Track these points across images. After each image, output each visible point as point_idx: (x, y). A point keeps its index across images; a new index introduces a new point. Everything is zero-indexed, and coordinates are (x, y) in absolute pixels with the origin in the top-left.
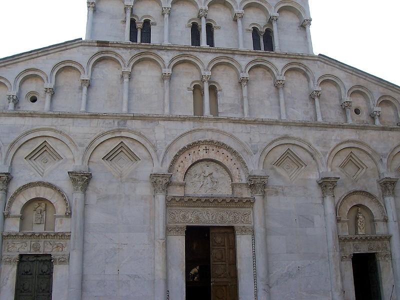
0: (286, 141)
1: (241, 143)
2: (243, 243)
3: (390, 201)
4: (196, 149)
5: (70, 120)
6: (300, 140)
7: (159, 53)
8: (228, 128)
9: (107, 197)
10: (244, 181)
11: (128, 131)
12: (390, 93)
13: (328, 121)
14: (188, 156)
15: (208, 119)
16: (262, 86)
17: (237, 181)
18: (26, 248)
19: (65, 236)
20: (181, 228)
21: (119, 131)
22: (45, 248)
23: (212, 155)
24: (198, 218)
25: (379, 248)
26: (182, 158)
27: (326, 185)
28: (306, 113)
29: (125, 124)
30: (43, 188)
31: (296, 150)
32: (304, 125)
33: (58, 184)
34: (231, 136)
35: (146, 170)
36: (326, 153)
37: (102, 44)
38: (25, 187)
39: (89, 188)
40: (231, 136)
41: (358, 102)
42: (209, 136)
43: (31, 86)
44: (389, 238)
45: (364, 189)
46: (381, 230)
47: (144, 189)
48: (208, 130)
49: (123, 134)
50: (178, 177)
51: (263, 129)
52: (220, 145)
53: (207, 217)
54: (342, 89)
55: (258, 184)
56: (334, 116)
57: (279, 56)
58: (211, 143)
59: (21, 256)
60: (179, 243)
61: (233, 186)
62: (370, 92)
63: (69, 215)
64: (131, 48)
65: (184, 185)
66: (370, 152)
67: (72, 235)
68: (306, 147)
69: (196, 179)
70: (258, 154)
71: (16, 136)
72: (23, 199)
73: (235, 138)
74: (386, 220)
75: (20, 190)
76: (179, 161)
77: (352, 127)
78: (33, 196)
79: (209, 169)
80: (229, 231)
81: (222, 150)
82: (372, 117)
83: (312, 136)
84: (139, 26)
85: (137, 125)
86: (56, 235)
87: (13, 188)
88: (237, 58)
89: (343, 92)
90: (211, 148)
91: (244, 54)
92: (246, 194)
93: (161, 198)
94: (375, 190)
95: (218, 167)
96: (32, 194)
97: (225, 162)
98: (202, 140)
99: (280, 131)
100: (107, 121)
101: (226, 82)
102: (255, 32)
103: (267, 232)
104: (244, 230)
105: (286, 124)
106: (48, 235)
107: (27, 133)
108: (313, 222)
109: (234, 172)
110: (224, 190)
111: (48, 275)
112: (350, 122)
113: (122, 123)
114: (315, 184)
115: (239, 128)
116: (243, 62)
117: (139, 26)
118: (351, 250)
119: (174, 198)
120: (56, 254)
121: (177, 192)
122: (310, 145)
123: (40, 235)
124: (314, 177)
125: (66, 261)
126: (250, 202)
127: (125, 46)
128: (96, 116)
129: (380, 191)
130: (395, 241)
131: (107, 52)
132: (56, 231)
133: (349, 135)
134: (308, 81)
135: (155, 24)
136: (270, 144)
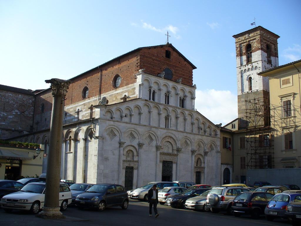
1: (176, 137)
2: (174, 166)
5: (138, 126)
6: (189, 137)
7: (160, 105)
8: (174, 132)
10: (176, 149)
11: (152, 131)
16: (181, 119)
18: (127, 164)
19: (137, 162)
21: (150, 131)
22: (132, 165)
23: (169, 140)
24: (165, 158)
27: (193, 152)
28: (190, 129)
31: (188, 141)
32: (191, 133)
33: (135, 146)
34: (174, 135)
35: (154, 143)
37: (146, 100)
40: (174, 135)
41: (202, 126)
42: (170, 135)
44: (204, 168)
47: (154, 149)
48: (169, 133)
49: (151, 132)
51: (182, 134)
52: (171, 137)
53: (168, 158)
55: (178, 150)
56: (195, 130)
57: (187, 110)
60: (161, 165)
61: (173, 150)
62: (206, 124)
63: (138, 156)
64: (153, 103)
66: (203, 143)
72: (126, 150)
73: (175, 136)
74: (204, 163)
77: (201, 135)
79: (168, 144)
80: (171, 162)
81: (171, 139)
82: (205, 131)
83: (192, 136)
86: (136, 161)
88: (177, 110)
90: (169, 138)
91: (179, 109)
96: (128, 148)
97: (172, 143)
99: (185, 134)
100: (147, 127)
102: (180, 99)
104: (175, 163)
105: (187, 133)
109: (174, 146)
111: (132, 173)
112: (201, 133)
116: (179, 111)
120: (135, 167)
121: (161, 151)
122: (191, 139)
124: (190, 149)
126: (177, 155)
130: (206, 169)
133: (200, 137)
134: (192, 118)
135: (156, 93)
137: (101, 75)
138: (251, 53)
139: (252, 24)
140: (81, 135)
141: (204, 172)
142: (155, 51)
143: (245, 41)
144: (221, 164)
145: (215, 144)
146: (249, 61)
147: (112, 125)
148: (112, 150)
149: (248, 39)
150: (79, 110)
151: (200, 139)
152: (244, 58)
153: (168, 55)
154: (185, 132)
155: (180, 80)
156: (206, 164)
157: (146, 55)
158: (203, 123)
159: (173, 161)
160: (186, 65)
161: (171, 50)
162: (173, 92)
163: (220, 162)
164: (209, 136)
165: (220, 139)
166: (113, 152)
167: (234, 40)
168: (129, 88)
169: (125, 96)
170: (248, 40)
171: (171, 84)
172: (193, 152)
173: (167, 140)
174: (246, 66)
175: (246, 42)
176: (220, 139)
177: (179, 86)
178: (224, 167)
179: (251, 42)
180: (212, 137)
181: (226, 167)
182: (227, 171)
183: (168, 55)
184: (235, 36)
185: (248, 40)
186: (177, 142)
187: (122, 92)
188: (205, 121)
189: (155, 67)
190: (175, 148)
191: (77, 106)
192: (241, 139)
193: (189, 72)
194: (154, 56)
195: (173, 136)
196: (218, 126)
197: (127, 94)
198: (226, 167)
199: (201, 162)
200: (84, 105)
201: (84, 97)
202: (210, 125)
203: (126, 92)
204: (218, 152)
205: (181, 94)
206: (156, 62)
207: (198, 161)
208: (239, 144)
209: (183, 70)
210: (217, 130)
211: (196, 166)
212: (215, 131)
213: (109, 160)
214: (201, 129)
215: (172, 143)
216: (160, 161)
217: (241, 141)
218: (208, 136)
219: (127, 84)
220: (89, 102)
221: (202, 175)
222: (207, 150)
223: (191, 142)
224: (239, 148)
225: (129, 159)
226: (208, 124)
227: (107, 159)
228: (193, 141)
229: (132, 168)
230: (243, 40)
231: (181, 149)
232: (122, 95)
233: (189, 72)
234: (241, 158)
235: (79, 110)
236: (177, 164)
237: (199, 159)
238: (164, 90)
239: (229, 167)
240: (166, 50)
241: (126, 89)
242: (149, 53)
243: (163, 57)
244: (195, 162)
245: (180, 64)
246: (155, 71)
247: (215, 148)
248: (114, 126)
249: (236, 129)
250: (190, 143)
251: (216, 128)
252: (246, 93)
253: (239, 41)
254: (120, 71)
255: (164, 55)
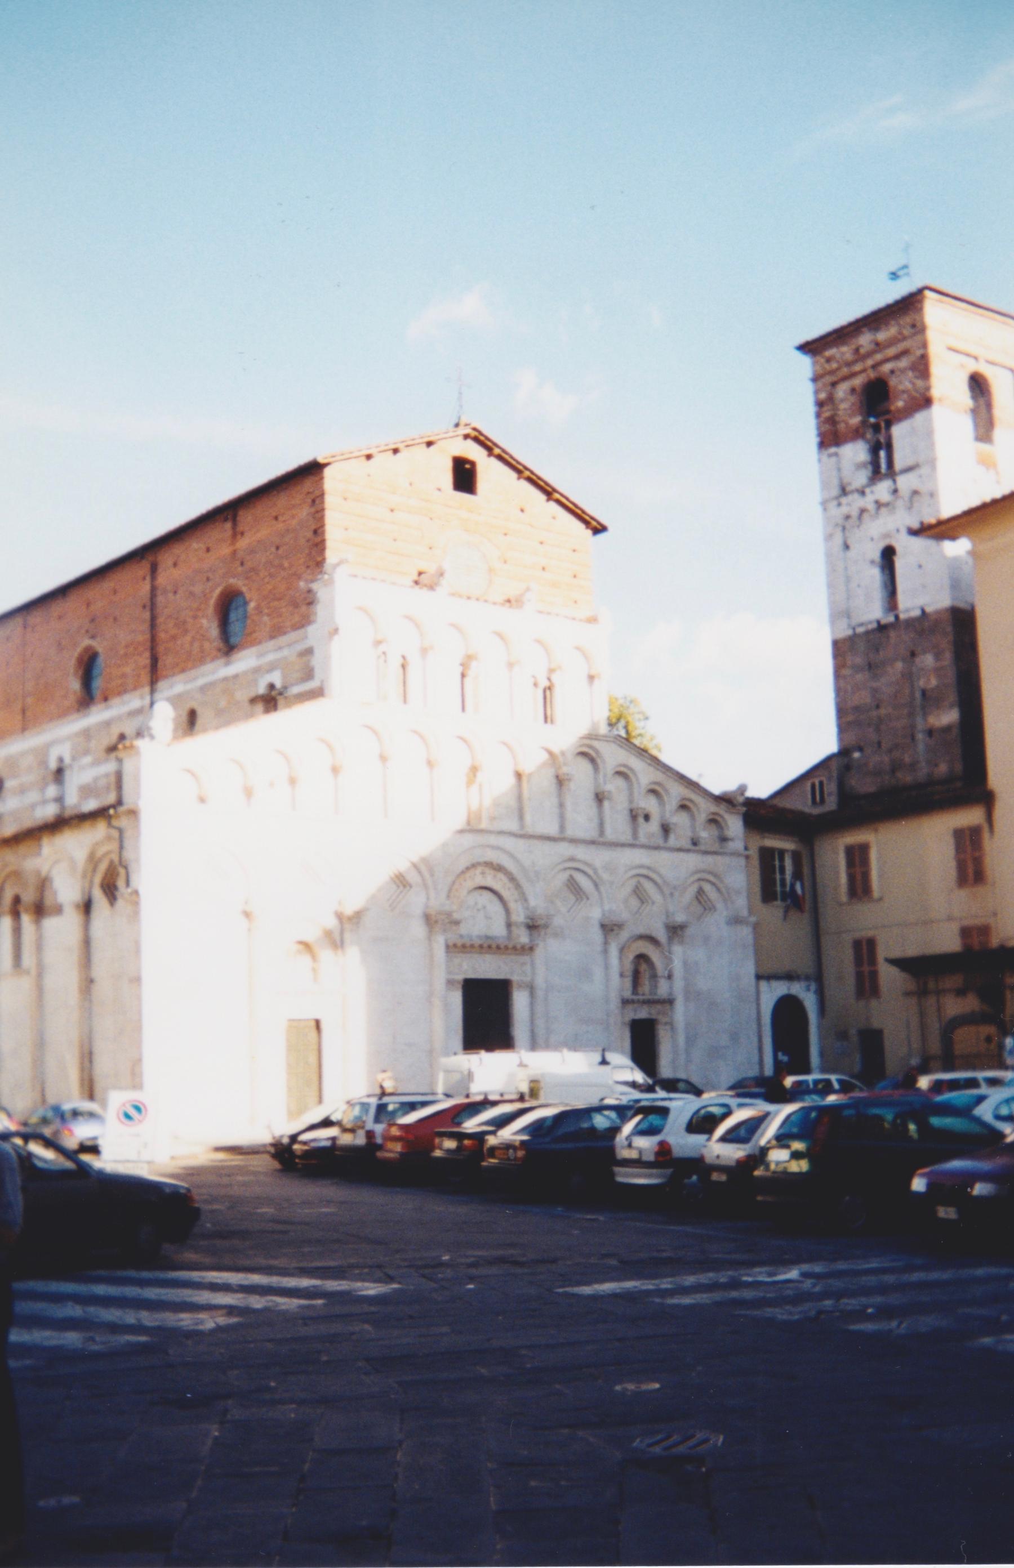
3: (678, 950)
4: (471, 872)
12: (693, 796)
23: (489, 882)
31: (580, 878)
32: (593, 842)
34: (512, 856)
41: (651, 805)
42: (491, 856)
44: (670, 1002)
45: (648, 932)
46: (663, 989)
47: (418, 929)
51: (548, 847)
52: (499, 868)
53: (488, 968)
54: (635, 785)
56: (618, 826)
58: (489, 864)
60: (457, 998)
61: (509, 925)
62: (666, 791)
68: (590, 872)
74: (670, 977)
77: (643, 846)
82: (666, 829)
83: (598, 858)
89: (636, 791)
92: (523, 937)
93: (440, 942)
94: (662, 935)
98: (481, 860)
99: (565, 850)
104: (521, 986)
105: (573, 841)
109: (512, 905)
112: (642, 839)
115: (521, 843)
124: (596, 914)
137: (154, 589)
138: (889, 424)
139: (894, 276)
140: (67, 890)
141: (671, 1024)
143: (858, 367)
144: (759, 977)
145: (720, 885)
146: (881, 464)
149: (869, 354)
150: (61, 760)
151: (642, 866)
152: (856, 452)
154: (562, 839)
156: (678, 984)
158: (653, 791)
159: (515, 978)
163: (749, 969)
164: (688, 851)
165: (747, 857)
167: (805, 364)
168: (286, 652)
169: (272, 686)
170: (870, 362)
172: (609, 928)
173: (480, 881)
174: (868, 490)
175: (864, 371)
176: (742, 861)
178: (771, 993)
179: (887, 367)
180: (706, 853)
181: (780, 989)
182: (788, 1016)
184: (808, 348)
185: (870, 362)
186: (523, 882)
187: (257, 671)
188: (659, 776)
190: (519, 916)
191: (48, 746)
192: (850, 851)
196: (725, 800)
197: (276, 678)
198: (780, 989)
199: (654, 976)
200: (87, 734)
201: (87, 698)
202: (693, 796)
203: (271, 668)
204: (736, 921)
207: (641, 969)
208: (843, 879)
210: (727, 816)
211: (628, 994)
212: (714, 821)
214: (647, 817)
215: (506, 894)
216: (450, 983)
217: (850, 863)
218: (680, 850)
219: (277, 631)
220: (108, 724)
221: (663, 1035)
222: (680, 918)
223: (596, 885)
224: (844, 898)
226: (676, 792)
228: (605, 876)
230: (849, 364)
231: (549, 917)
232: (255, 682)
234: (857, 944)
235: (61, 760)
236: (531, 988)
237: (642, 958)
239: (797, 989)
241: (271, 657)
244: (622, 975)
247: (720, 906)
249: (831, 804)
251: (721, 809)
252: (870, 627)
253: (827, 367)
254: (240, 569)
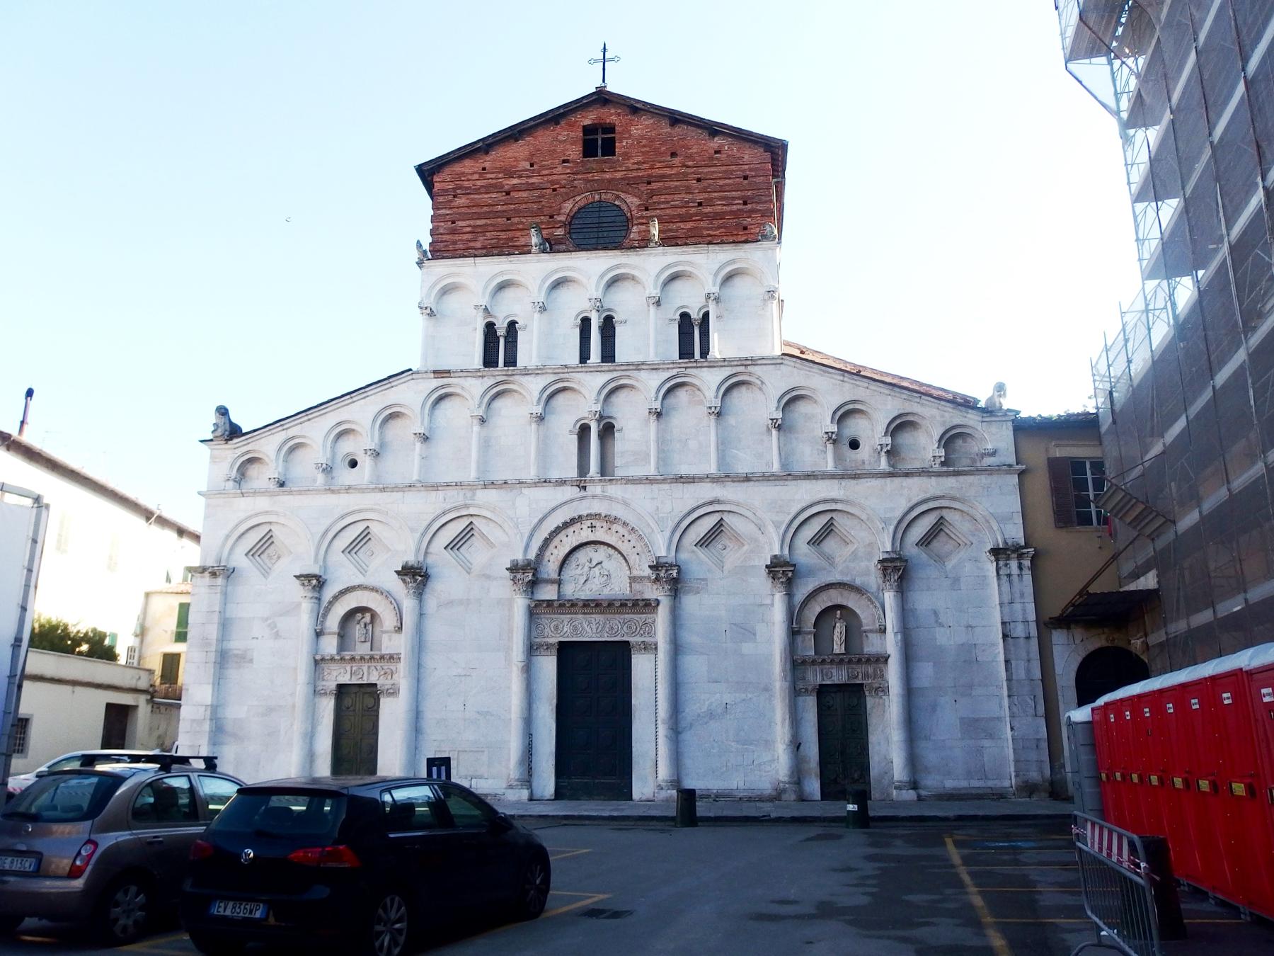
0: (717, 507)
4: (576, 527)
9: (450, 603)
11: (480, 507)
12: (916, 408)
13: (797, 468)
14: (564, 539)
15: (592, 481)
17: (636, 573)
19: (392, 658)
20: (552, 645)
21: (466, 506)
23: (600, 535)
25: (867, 676)
26: (556, 541)
29: (474, 494)
30: (366, 593)
36: (781, 523)
37: (438, 373)
38: (343, 592)
39: (427, 590)
40: (626, 504)
43: (348, 447)
44: (883, 659)
45: (846, 579)
46: (872, 645)
50: (550, 567)
52: (610, 520)
53: (590, 629)
59: (341, 687)
61: (633, 579)
65: (559, 583)
67: (402, 656)
69: (579, 571)
70: (668, 533)
71: (327, 522)
72: (340, 610)
75: (336, 598)
76: (552, 546)
78: (354, 605)
84: (501, 330)
85: (492, 495)
86: (382, 657)
87: (329, 593)
88: (643, 375)
90: (597, 524)
91: (655, 368)
92: (652, 592)
95: (611, 551)
97: (619, 545)
99: (707, 491)
101: (631, 415)
103: (677, 649)
106: (372, 658)
107: (343, 517)
108: (755, 635)
109: (633, 558)
110: (619, 587)
113: (469, 494)
114: (764, 572)
117: (501, 330)
118: (815, 677)
119: (540, 603)
121: (547, 593)
123: (362, 658)
125: (394, 692)
127: (473, 373)
128: (436, 487)
129: (880, 581)
131: (448, 385)
132: (383, 652)
136: (689, 514)
141: (884, 690)
142: (518, 152)
145: (971, 511)
147: (267, 512)
148: (267, 619)
153: (598, 142)
155: (655, 230)
157: (466, 184)
160: (716, 152)
161: (611, 116)
162: (626, 304)
166: (273, 626)
171: (590, 267)
176: (1015, 479)
177: (651, 264)
183: (598, 142)
189: (515, 220)
193: (746, 178)
194: (509, 174)
195: (617, 511)
205: (690, 299)
206: (524, 194)
209: (699, 180)
213: (251, 661)
225: (363, 649)
227: (244, 659)
229: (371, 693)
233: (746, 178)
236: (651, 648)
238: (576, 303)
240: (587, 122)
242: (484, 169)
243: (564, 161)
245: (676, 161)
246: (518, 234)
248: (277, 514)
250: (756, 529)
255: (575, 152)
